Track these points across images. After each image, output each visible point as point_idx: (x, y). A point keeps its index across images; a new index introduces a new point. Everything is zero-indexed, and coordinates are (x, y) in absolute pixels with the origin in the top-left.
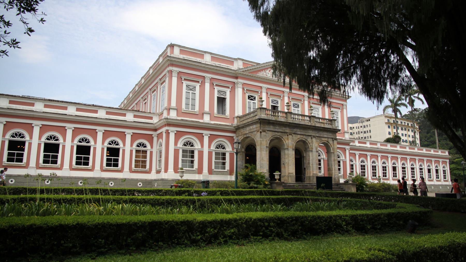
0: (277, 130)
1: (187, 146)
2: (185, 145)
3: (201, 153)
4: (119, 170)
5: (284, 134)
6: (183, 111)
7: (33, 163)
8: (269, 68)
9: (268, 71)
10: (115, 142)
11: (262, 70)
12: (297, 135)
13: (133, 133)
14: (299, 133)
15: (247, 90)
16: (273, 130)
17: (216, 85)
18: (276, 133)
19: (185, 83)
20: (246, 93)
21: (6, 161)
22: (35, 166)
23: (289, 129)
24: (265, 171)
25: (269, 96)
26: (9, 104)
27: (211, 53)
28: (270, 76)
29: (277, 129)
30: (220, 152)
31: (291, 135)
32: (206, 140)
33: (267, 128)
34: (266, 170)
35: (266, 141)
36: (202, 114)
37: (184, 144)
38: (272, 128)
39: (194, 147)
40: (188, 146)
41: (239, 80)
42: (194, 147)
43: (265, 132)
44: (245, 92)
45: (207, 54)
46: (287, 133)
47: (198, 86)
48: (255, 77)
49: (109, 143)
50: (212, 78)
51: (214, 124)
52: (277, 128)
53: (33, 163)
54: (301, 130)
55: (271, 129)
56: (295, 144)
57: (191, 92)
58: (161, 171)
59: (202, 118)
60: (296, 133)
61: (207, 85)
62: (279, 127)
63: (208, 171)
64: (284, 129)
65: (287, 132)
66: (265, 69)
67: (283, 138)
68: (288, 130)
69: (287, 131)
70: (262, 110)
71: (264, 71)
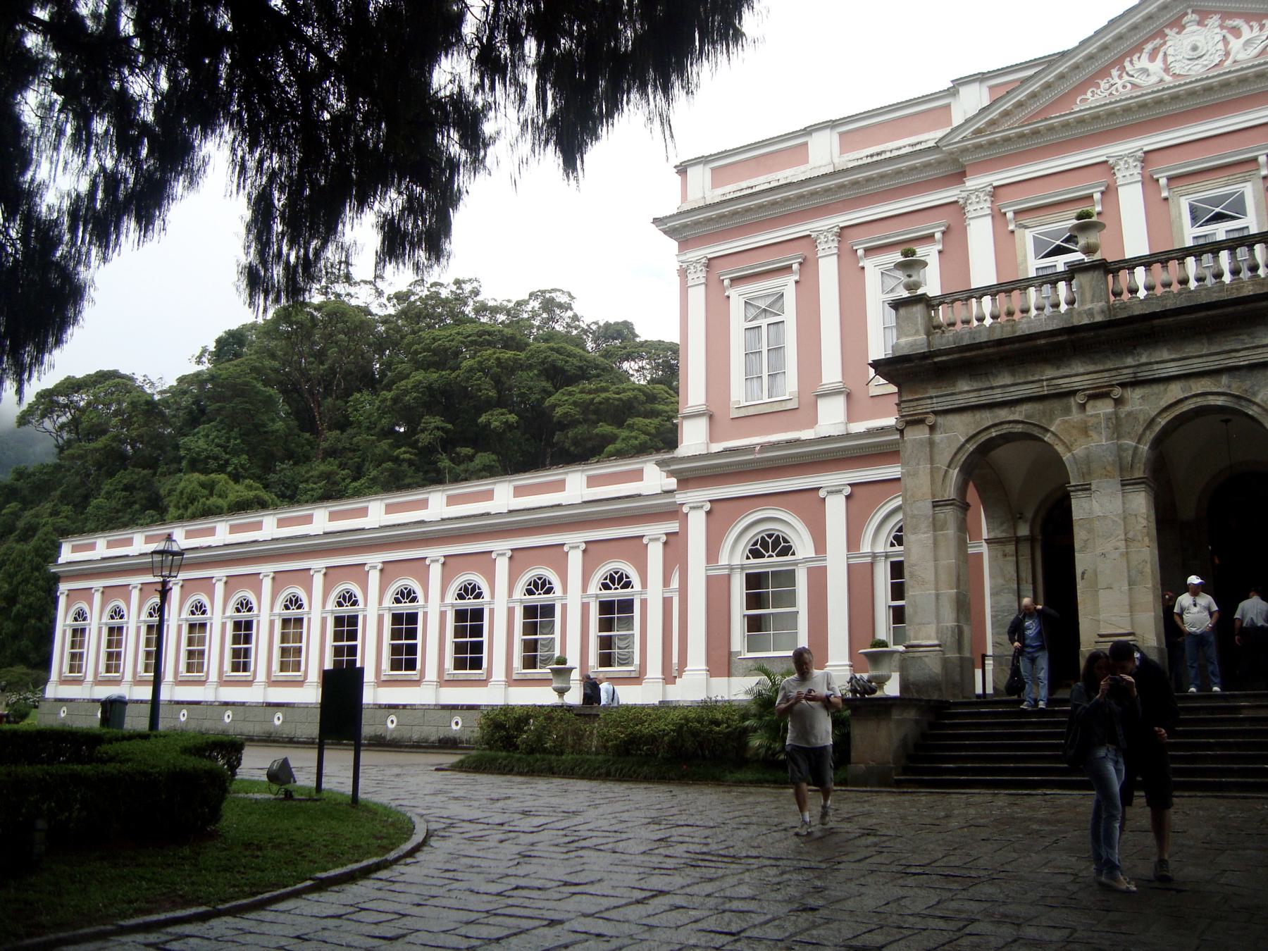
0: (998, 396)
1: (763, 556)
2: (756, 554)
3: (818, 578)
4: (633, 675)
5: (1057, 405)
6: (734, 414)
7: (431, 674)
8: (1146, 41)
9: (1145, 56)
10: (621, 578)
11: (1104, 72)
12: (1156, 388)
13: (667, 534)
14: (1172, 369)
15: (1016, 213)
16: (973, 399)
17: (869, 251)
18: (1004, 414)
19: (737, 297)
20: (1018, 232)
21: (230, 669)
22: (171, 679)
23: (1091, 368)
24: (929, 638)
25: (1165, 194)
26: (330, 520)
27: (832, 125)
28: (1161, 81)
29: (1004, 385)
30: (770, 570)
31: (1106, 395)
32: (836, 510)
33: (934, 398)
34: (933, 634)
35: (933, 471)
36: (805, 410)
37: (751, 551)
38: (965, 390)
39: (793, 554)
40: (771, 556)
41: (972, 183)
42: (793, 554)
43: (921, 426)
44: (1011, 227)
45: (814, 135)
46: (1073, 393)
47: (787, 285)
48: (1066, 125)
49: (603, 584)
50: (842, 228)
51: (870, 433)
52: (1007, 379)
53: (431, 674)
54: (1191, 350)
55: (961, 401)
56: (1144, 448)
57: (764, 322)
58: (83, 681)
59: (813, 422)
60: (1145, 374)
61: (828, 269)
62: (1013, 375)
63: (708, 662)
64: (1050, 373)
65: (1077, 386)
66: (1118, 62)
67: (1047, 430)
68: (1078, 375)
69: (1076, 382)
70: (902, 311)
71: (1115, 72)
